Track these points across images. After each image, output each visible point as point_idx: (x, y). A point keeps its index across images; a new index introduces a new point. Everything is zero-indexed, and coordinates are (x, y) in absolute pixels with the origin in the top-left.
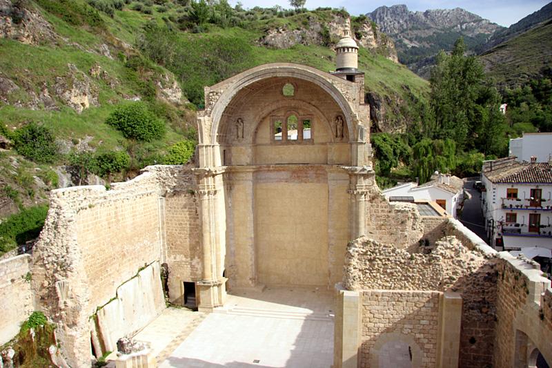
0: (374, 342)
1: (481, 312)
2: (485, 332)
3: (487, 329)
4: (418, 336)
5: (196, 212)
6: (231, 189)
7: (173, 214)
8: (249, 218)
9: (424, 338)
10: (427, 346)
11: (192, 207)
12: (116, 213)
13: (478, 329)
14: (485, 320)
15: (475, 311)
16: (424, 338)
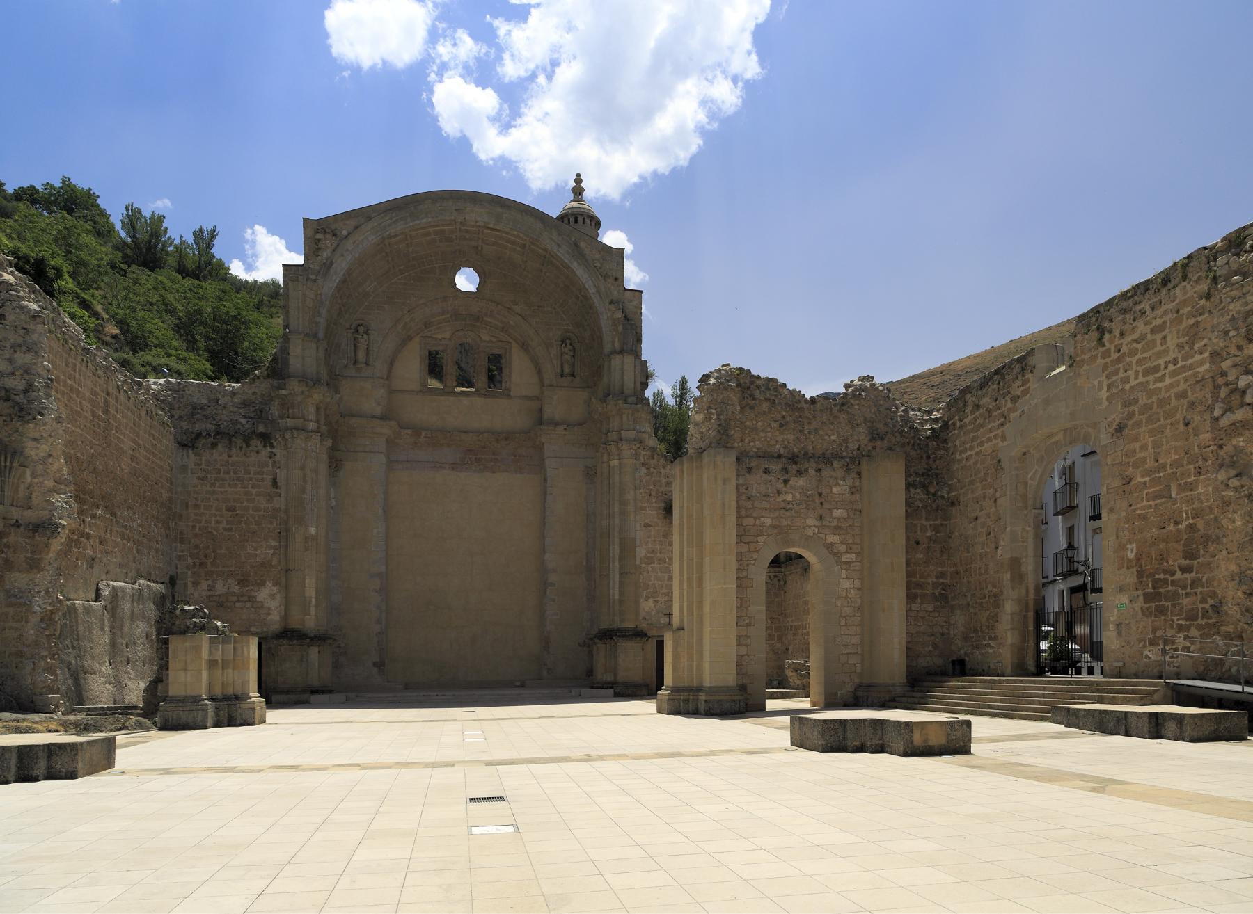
0: (755, 555)
1: (928, 493)
2: (936, 529)
3: (938, 522)
4: (830, 539)
5: (275, 480)
6: (337, 468)
7: (213, 485)
8: (375, 531)
9: (841, 543)
10: (846, 558)
11: (265, 470)
12: (106, 402)
13: (925, 523)
14: (934, 506)
15: (918, 491)
16: (841, 543)
